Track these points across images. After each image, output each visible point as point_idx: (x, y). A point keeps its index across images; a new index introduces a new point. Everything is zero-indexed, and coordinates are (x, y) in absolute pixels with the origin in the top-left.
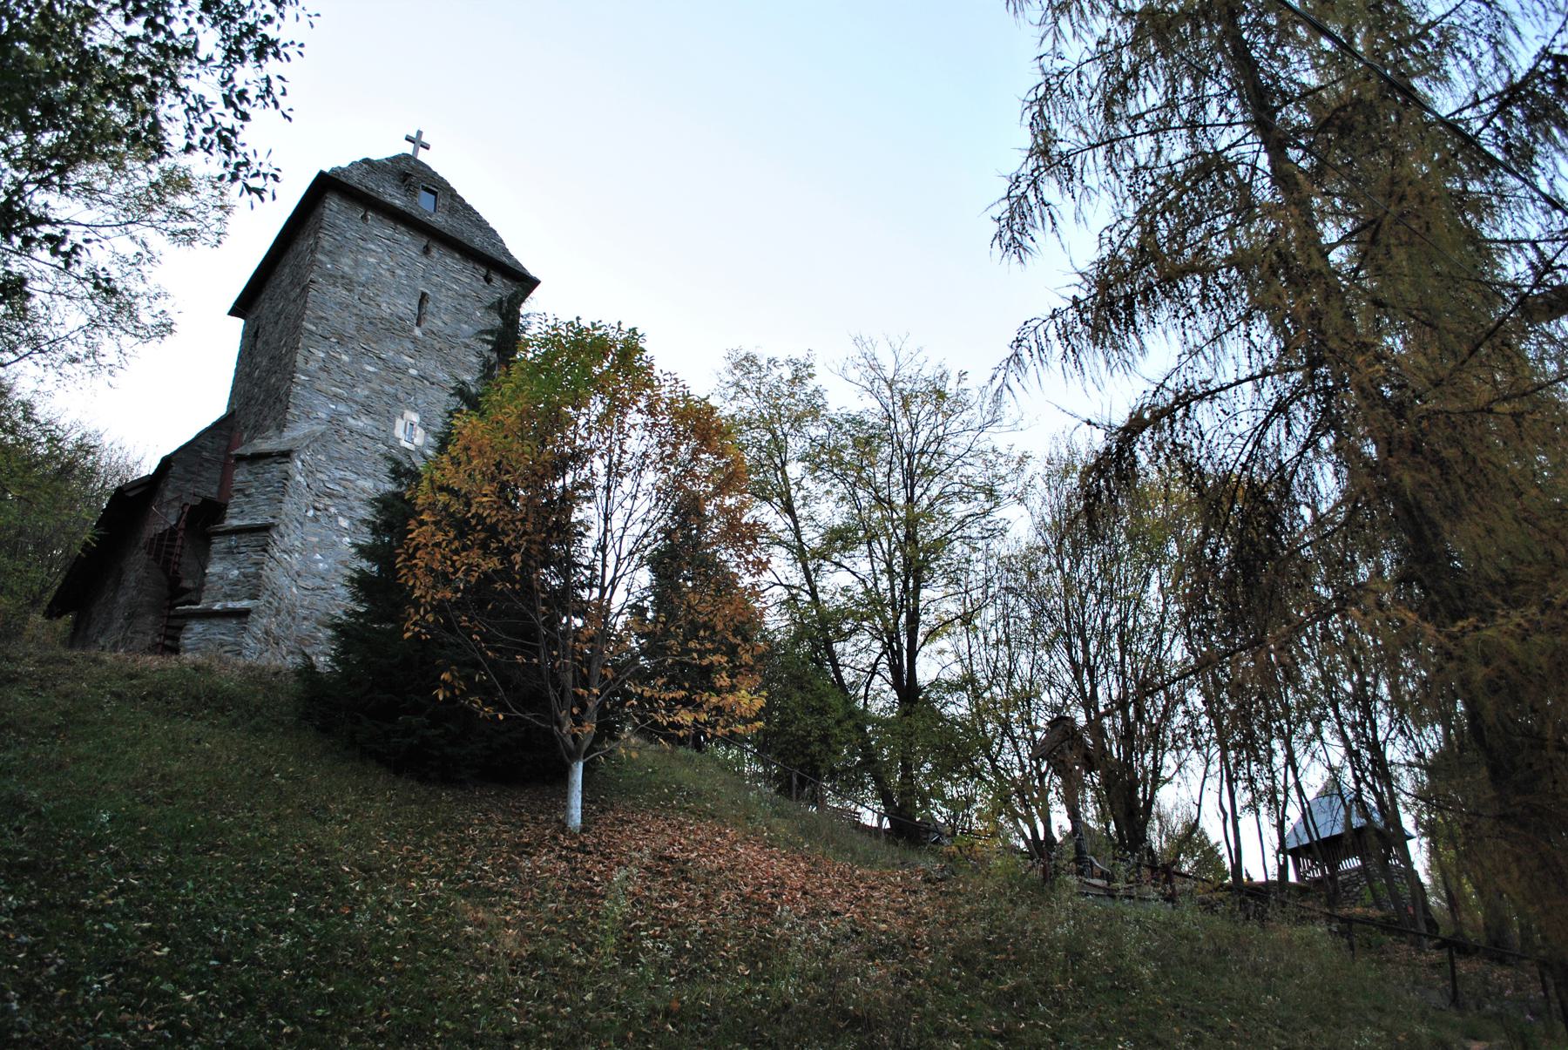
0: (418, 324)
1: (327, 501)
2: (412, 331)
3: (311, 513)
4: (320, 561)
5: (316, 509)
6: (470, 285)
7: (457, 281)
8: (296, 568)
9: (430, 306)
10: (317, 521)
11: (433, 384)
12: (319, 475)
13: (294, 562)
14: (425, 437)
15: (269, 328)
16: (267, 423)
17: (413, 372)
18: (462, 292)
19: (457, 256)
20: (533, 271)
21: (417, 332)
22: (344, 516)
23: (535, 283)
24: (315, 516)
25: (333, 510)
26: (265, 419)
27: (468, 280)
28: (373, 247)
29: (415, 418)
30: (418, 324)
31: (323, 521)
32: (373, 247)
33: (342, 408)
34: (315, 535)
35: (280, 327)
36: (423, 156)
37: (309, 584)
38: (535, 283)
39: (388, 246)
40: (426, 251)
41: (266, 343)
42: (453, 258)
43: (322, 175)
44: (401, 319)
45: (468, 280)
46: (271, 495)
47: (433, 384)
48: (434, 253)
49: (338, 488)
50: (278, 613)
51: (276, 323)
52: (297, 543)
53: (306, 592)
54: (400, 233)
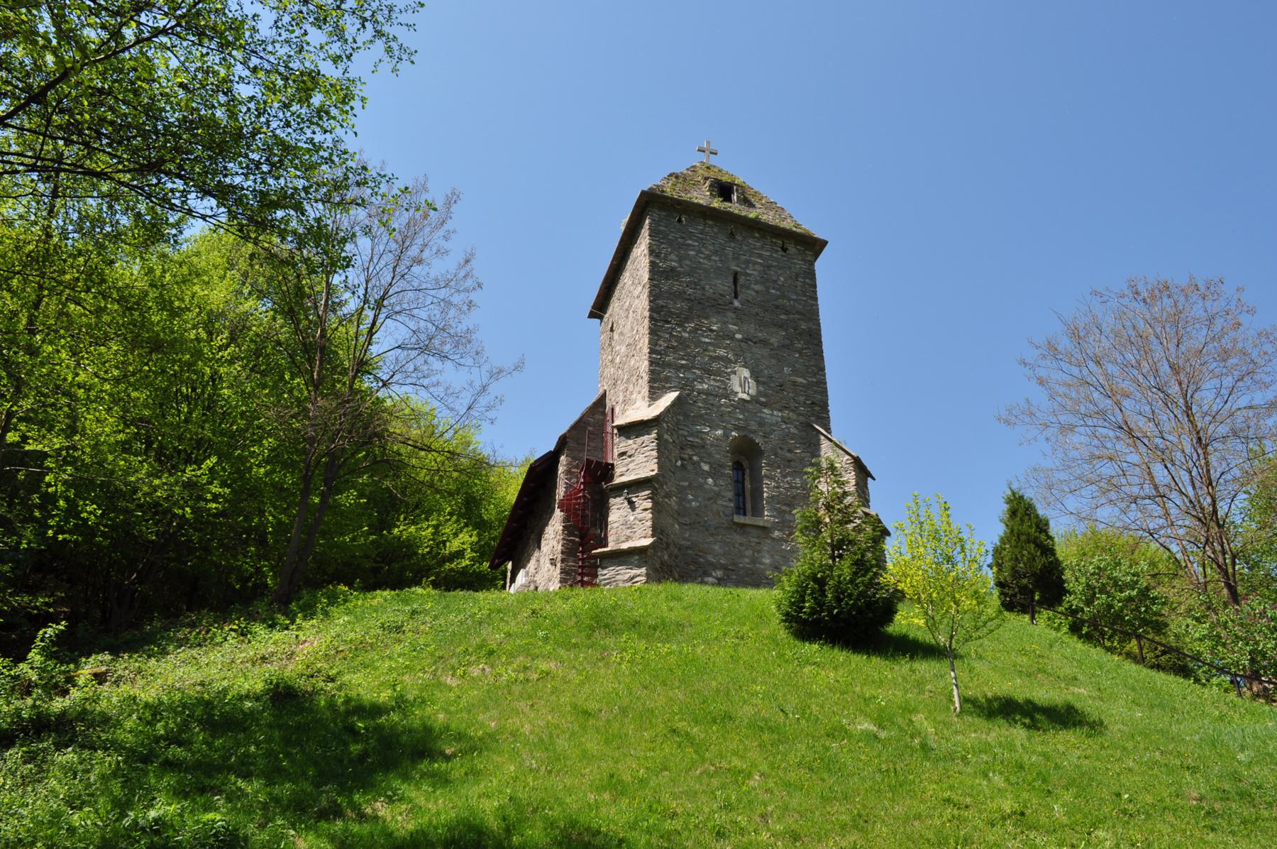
0: (736, 297)
1: (690, 452)
2: (732, 303)
3: (679, 463)
4: (693, 500)
5: (682, 459)
7: (760, 256)
8: (676, 507)
9: (742, 280)
10: (686, 468)
11: (755, 343)
12: (681, 432)
13: (673, 504)
15: (622, 322)
16: (634, 396)
17: (738, 336)
19: (757, 235)
20: (819, 234)
21: (736, 303)
22: (705, 462)
23: (824, 243)
24: (682, 465)
25: (695, 458)
26: (632, 393)
28: (690, 242)
29: (746, 373)
30: (736, 297)
31: (690, 467)
32: (690, 242)
34: (684, 480)
35: (630, 319)
36: (713, 160)
37: (686, 520)
38: (824, 243)
39: (702, 239)
40: (732, 235)
41: (621, 333)
42: (754, 238)
43: (643, 193)
44: (722, 295)
45: (768, 254)
46: (648, 454)
47: (755, 343)
48: (739, 238)
50: (668, 545)
51: (627, 317)
52: (673, 489)
54: (711, 227)
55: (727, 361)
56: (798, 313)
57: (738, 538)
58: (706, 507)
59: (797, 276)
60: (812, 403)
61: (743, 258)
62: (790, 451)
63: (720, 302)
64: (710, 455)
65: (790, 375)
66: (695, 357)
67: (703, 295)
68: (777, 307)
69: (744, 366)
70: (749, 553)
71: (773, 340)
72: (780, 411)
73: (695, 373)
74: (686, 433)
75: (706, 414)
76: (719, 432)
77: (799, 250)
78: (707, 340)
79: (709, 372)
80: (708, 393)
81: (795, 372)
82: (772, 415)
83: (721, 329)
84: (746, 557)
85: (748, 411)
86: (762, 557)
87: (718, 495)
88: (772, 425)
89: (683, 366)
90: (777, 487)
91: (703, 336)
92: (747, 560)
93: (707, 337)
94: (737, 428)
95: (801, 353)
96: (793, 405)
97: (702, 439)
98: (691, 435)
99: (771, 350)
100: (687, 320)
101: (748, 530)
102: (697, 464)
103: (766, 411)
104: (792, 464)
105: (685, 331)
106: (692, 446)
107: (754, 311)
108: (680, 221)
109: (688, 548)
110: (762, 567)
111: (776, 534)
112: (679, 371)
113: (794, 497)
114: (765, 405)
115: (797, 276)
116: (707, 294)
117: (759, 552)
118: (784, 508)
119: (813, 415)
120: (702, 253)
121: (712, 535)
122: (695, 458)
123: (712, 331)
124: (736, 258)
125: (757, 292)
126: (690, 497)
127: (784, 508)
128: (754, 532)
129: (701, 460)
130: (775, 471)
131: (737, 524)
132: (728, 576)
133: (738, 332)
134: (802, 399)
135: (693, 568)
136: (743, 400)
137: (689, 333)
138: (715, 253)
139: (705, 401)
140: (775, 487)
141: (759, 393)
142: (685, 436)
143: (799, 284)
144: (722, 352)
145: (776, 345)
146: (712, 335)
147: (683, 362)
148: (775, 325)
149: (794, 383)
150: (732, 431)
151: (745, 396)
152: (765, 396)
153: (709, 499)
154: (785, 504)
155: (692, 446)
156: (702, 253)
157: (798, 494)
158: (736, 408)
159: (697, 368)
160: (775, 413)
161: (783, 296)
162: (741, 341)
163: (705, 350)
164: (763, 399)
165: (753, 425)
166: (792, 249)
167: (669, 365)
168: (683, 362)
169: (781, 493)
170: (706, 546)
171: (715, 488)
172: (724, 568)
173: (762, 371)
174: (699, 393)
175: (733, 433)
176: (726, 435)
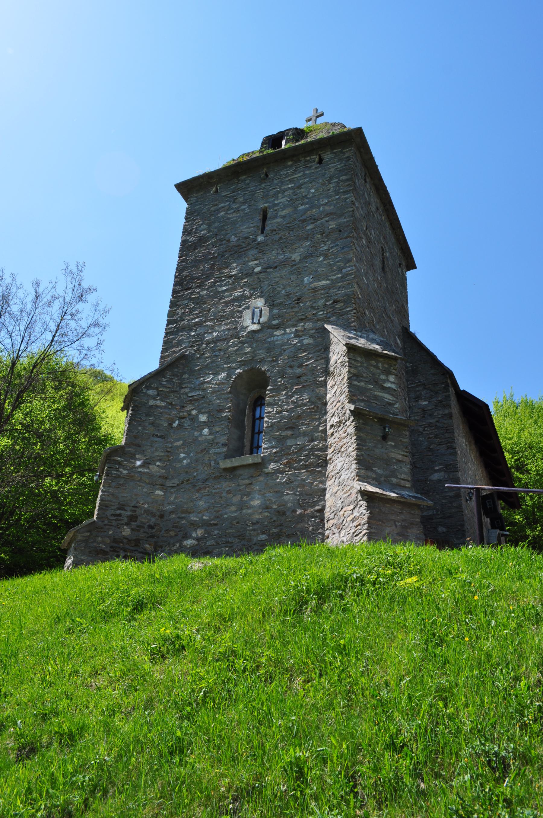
4: (184, 458)
6: (304, 175)
7: (291, 181)
11: (276, 267)
12: (183, 391)
14: (270, 312)
18: (297, 184)
19: (290, 163)
22: (203, 413)
24: (179, 425)
27: (300, 174)
28: (222, 205)
29: (260, 303)
30: (262, 232)
32: (222, 205)
33: (200, 330)
34: (178, 440)
44: (246, 238)
45: (300, 174)
47: (276, 267)
48: (271, 176)
49: (197, 393)
53: (172, 490)
55: (243, 298)
56: (327, 215)
57: (225, 485)
58: (197, 461)
59: (331, 178)
60: (335, 302)
61: (272, 192)
62: (301, 366)
63: (244, 245)
64: (210, 403)
65: (311, 283)
66: (210, 309)
67: (228, 246)
68: (304, 221)
69: (259, 297)
70: (236, 499)
71: (296, 256)
72: (295, 325)
73: (207, 325)
74: (187, 390)
75: (212, 362)
76: (223, 375)
77: (335, 153)
78: (224, 288)
79: (220, 319)
80: (216, 341)
81: (317, 278)
82: (284, 334)
83: (240, 271)
84: (233, 505)
85: (257, 341)
86: (252, 499)
87: (212, 443)
88: (283, 345)
89: (196, 324)
90: (281, 412)
91: (221, 286)
92: (233, 508)
93: (225, 285)
94: (242, 364)
95: (326, 256)
96: (309, 314)
97: (204, 390)
98: (193, 389)
99: (293, 266)
100: (208, 278)
101: (238, 472)
102: (194, 419)
103: (277, 333)
104: (302, 379)
105: (203, 290)
106: (193, 401)
107: (276, 237)
108: (217, 190)
109: (171, 512)
110: (250, 511)
111: (272, 466)
112: (191, 330)
113: (299, 417)
114: (277, 327)
115: (331, 178)
116: (231, 244)
117: (248, 494)
118: (284, 433)
119: (334, 314)
120: (232, 209)
121: (198, 491)
122: (194, 412)
123: (230, 277)
124: (265, 197)
125: (283, 217)
126: (183, 455)
127: (284, 433)
128: (245, 473)
129: (200, 412)
130: (280, 394)
131: (226, 470)
132: (208, 533)
133: (257, 265)
134: (321, 302)
135: (172, 533)
136: (254, 332)
137: (207, 290)
138: (244, 203)
139: (213, 350)
140: (277, 413)
141: (272, 317)
142: (186, 394)
143: (331, 186)
144: (237, 293)
145: (297, 259)
146: (231, 281)
147: (197, 320)
148: (299, 240)
149: (315, 290)
150: (237, 369)
151: (255, 327)
152: (278, 317)
153: (202, 451)
154: (286, 429)
155: (193, 401)
156: (232, 209)
157: (304, 411)
158: (244, 344)
159: (211, 320)
160: (288, 330)
161: (312, 207)
162: (260, 272)
163: (221, 299)
164: (275, 322)
165: (262, 353)
166: (327, 156)
167: (183, 329)
168: (197, 320)
169: (283, 417)
170: (191, 505)
171: (211, 437)
172: (206, 524)
173: (278, 293)
174: (207, 344)
175: (238, 371)
176: (229, 376)
